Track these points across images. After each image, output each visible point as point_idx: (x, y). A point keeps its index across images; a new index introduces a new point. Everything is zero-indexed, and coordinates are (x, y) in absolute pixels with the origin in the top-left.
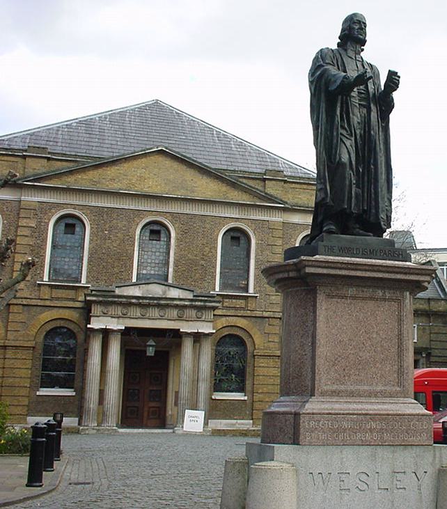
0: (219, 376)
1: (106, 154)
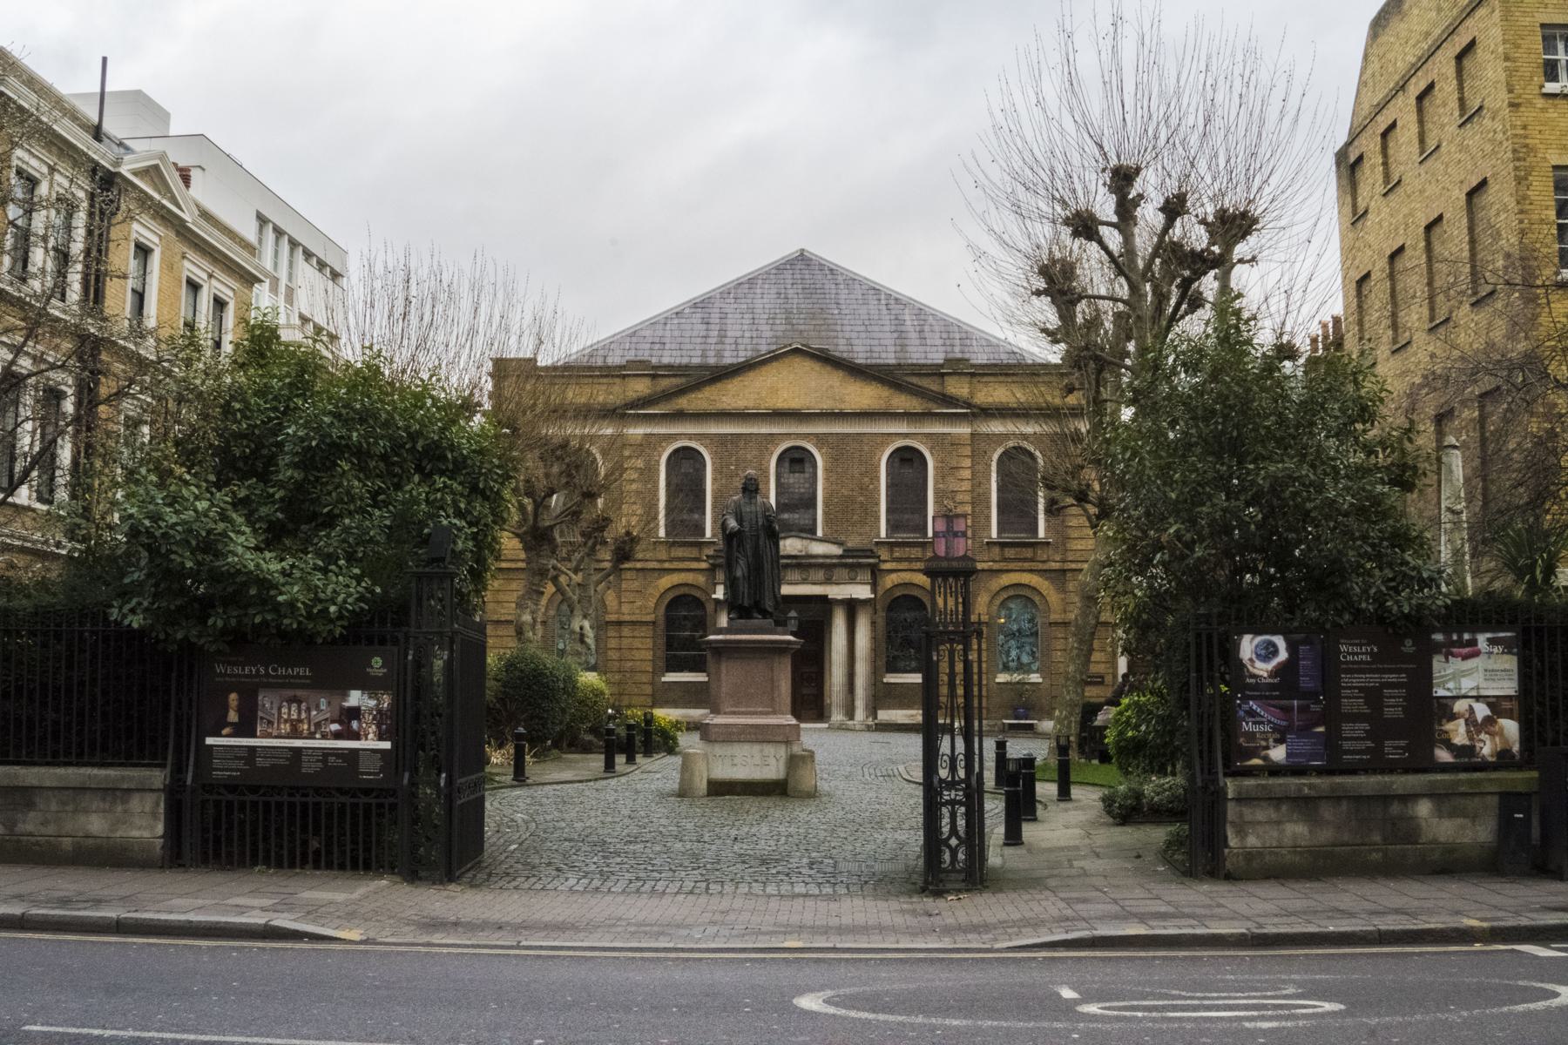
1: (729, 359)
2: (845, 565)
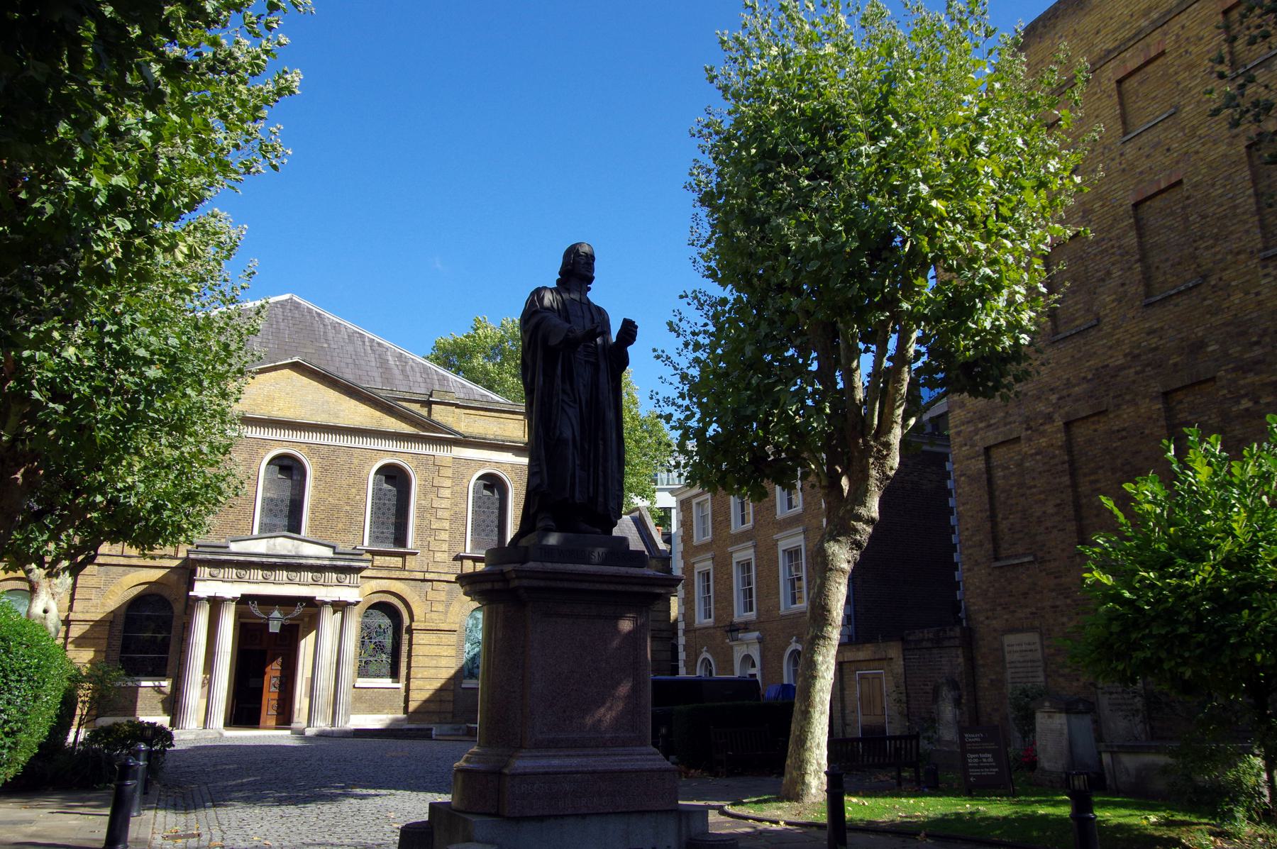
0: (365, 657)
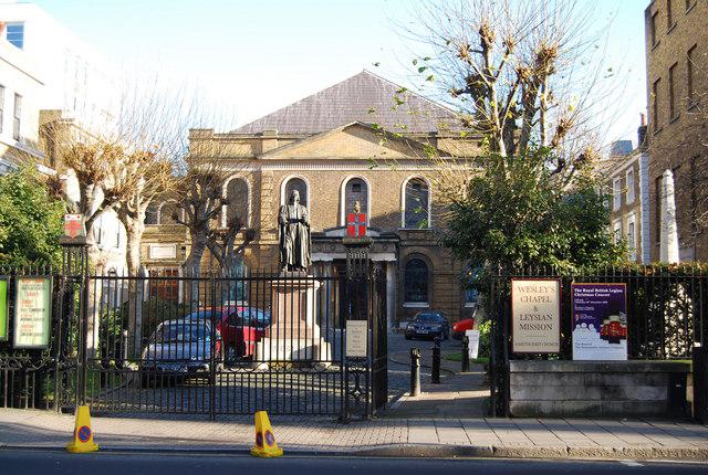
2: (381, 243)
